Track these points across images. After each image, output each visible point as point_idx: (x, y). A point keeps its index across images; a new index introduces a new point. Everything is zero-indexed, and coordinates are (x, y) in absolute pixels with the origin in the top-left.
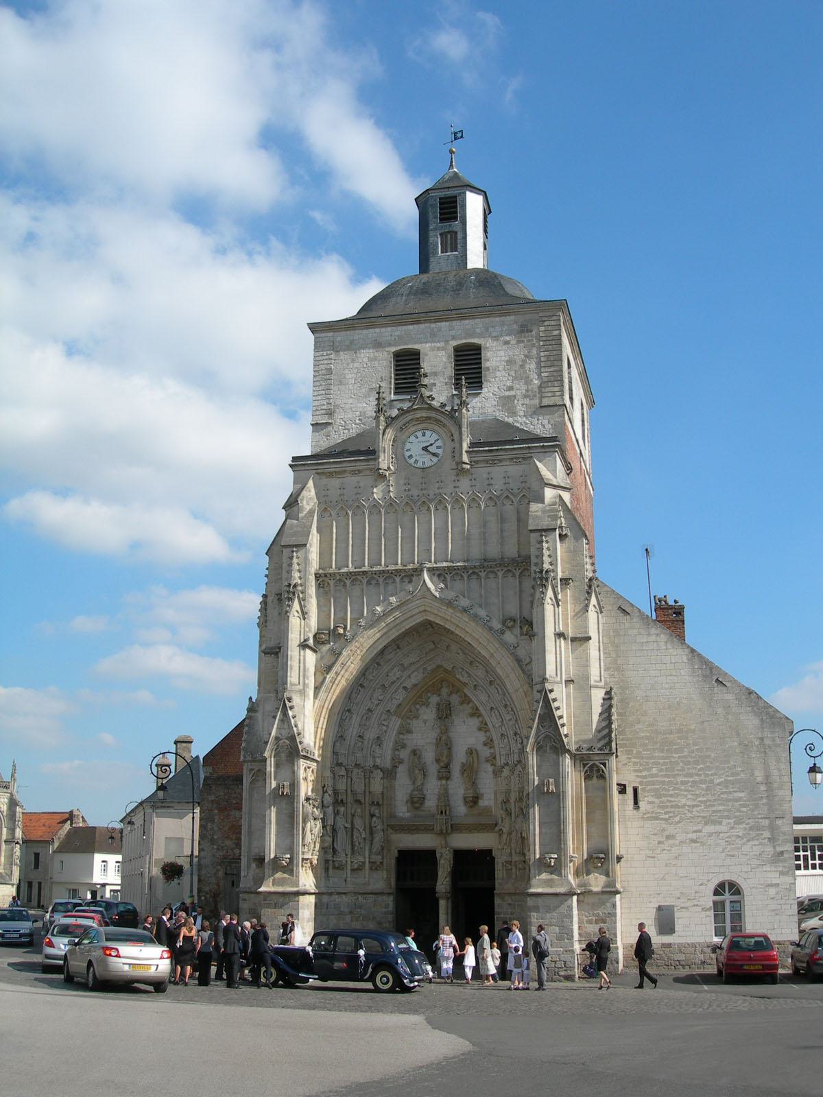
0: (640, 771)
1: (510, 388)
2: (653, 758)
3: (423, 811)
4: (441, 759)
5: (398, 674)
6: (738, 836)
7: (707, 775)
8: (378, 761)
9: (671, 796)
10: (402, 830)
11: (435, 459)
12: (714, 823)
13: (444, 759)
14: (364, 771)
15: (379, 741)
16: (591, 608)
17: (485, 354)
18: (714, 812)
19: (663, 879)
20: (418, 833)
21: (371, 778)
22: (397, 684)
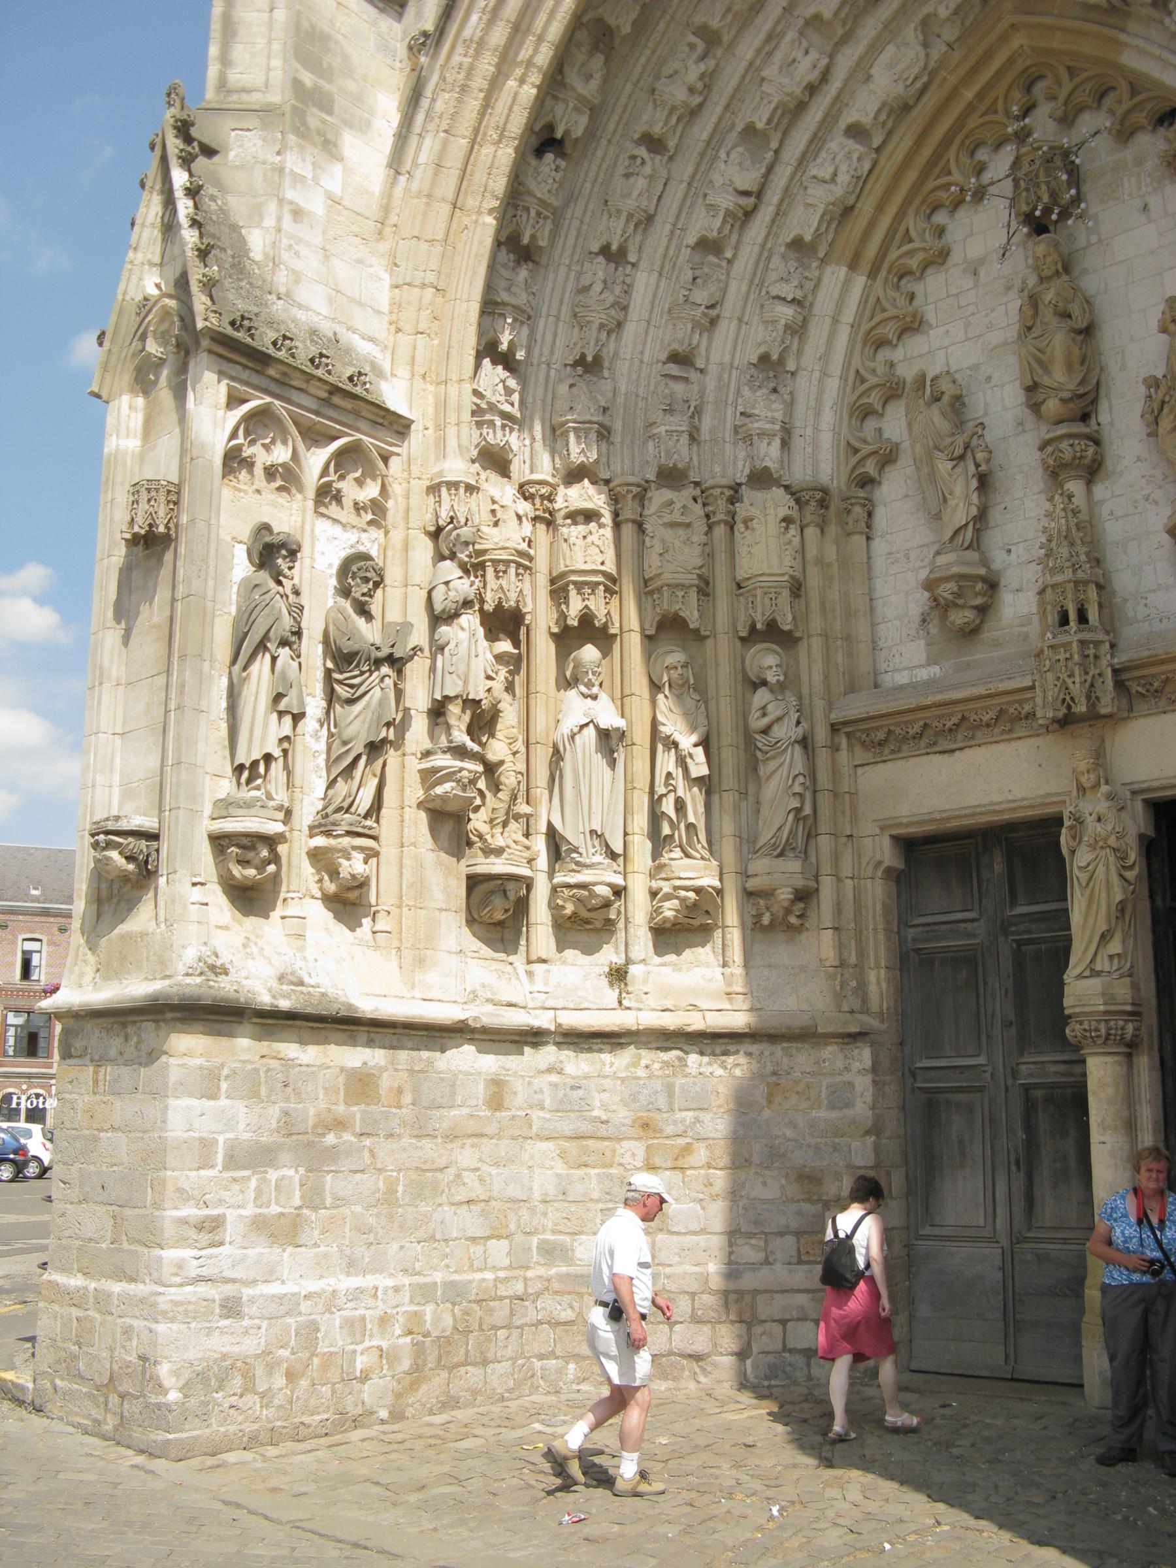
3: (997, 644)
4: (1046, 381)
8: (770, 454)
10: (905, 739)
13: (1059, 376)
14: (704, 495)
15: (771, 368)
20: (971, 742)
21: (739, 527)
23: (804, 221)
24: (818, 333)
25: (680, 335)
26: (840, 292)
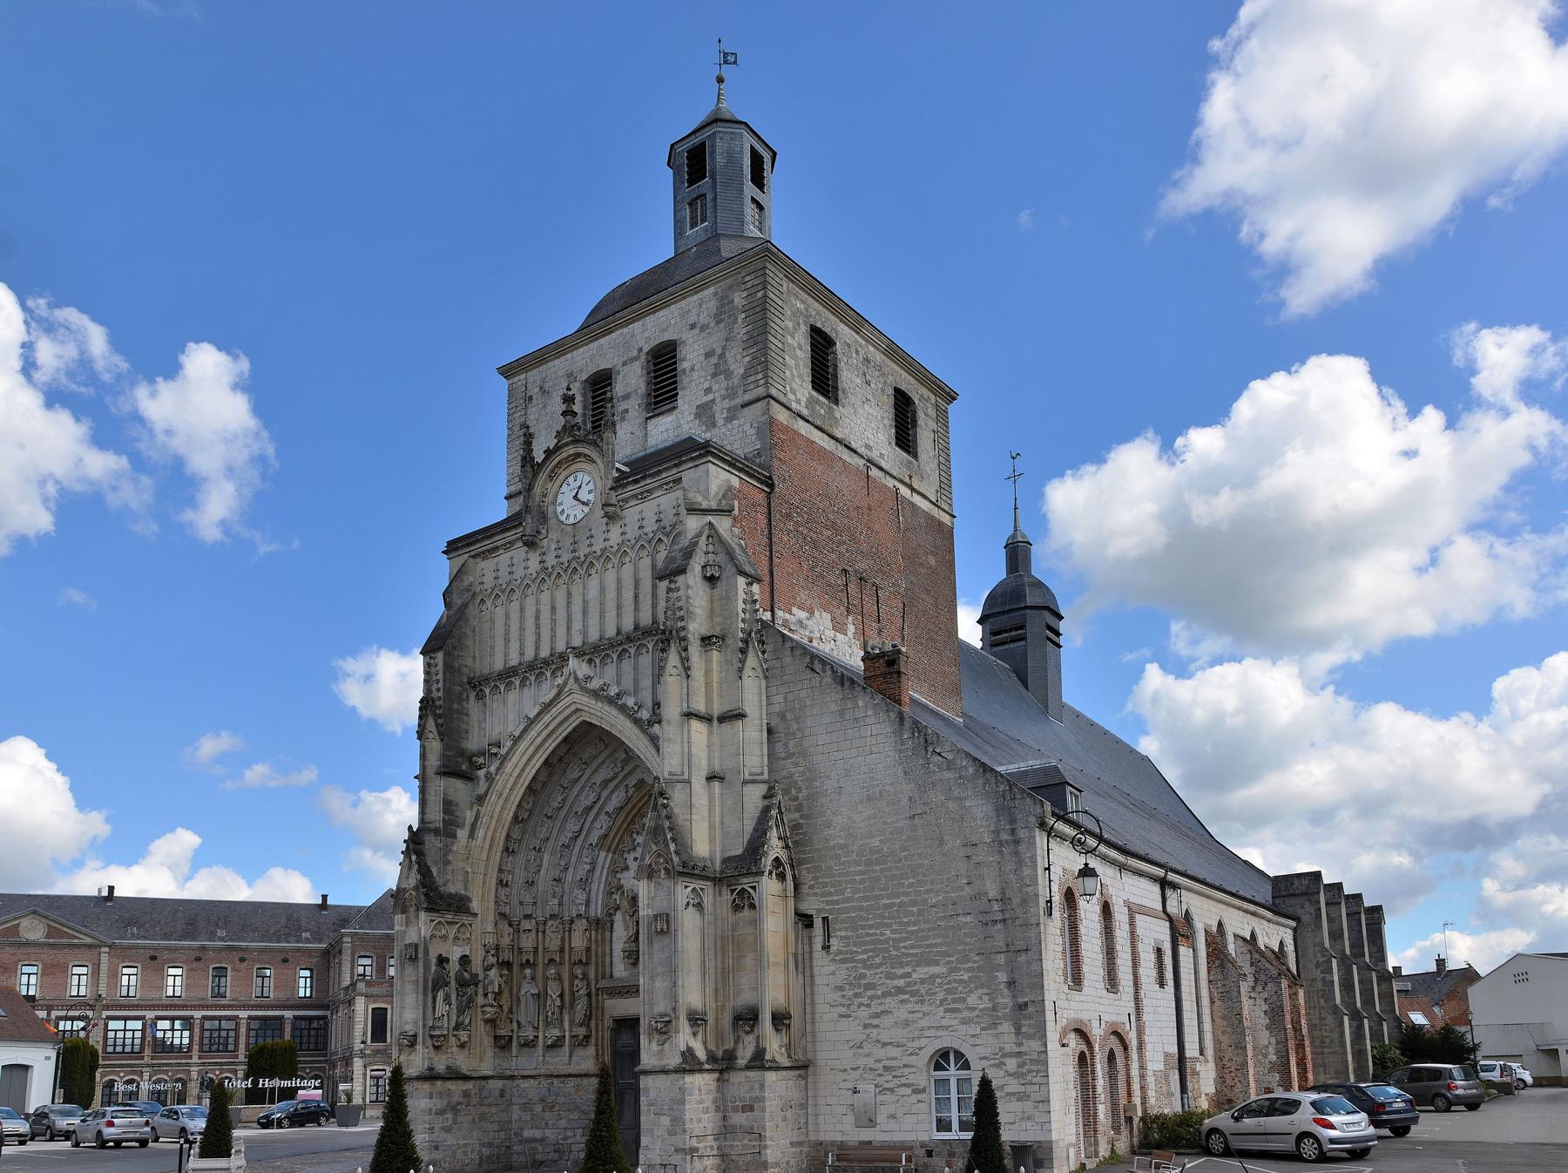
0: (831, 894)
1: (708, 391)
2: (847, 874)
5: (592, 797)
6: (961, 981)
7: (918, 893)
9: (871, 927)
11: (586, 509)
12: (929, 963)
15: (584, 883)
16: (747, 672)
17: (682, 352)
18: (928, 946)
19: (861, 1047)
22: (595, 810)
23: (594, 839)
24: (597, 873)
25: (557, 873)
26: (604, 859)
